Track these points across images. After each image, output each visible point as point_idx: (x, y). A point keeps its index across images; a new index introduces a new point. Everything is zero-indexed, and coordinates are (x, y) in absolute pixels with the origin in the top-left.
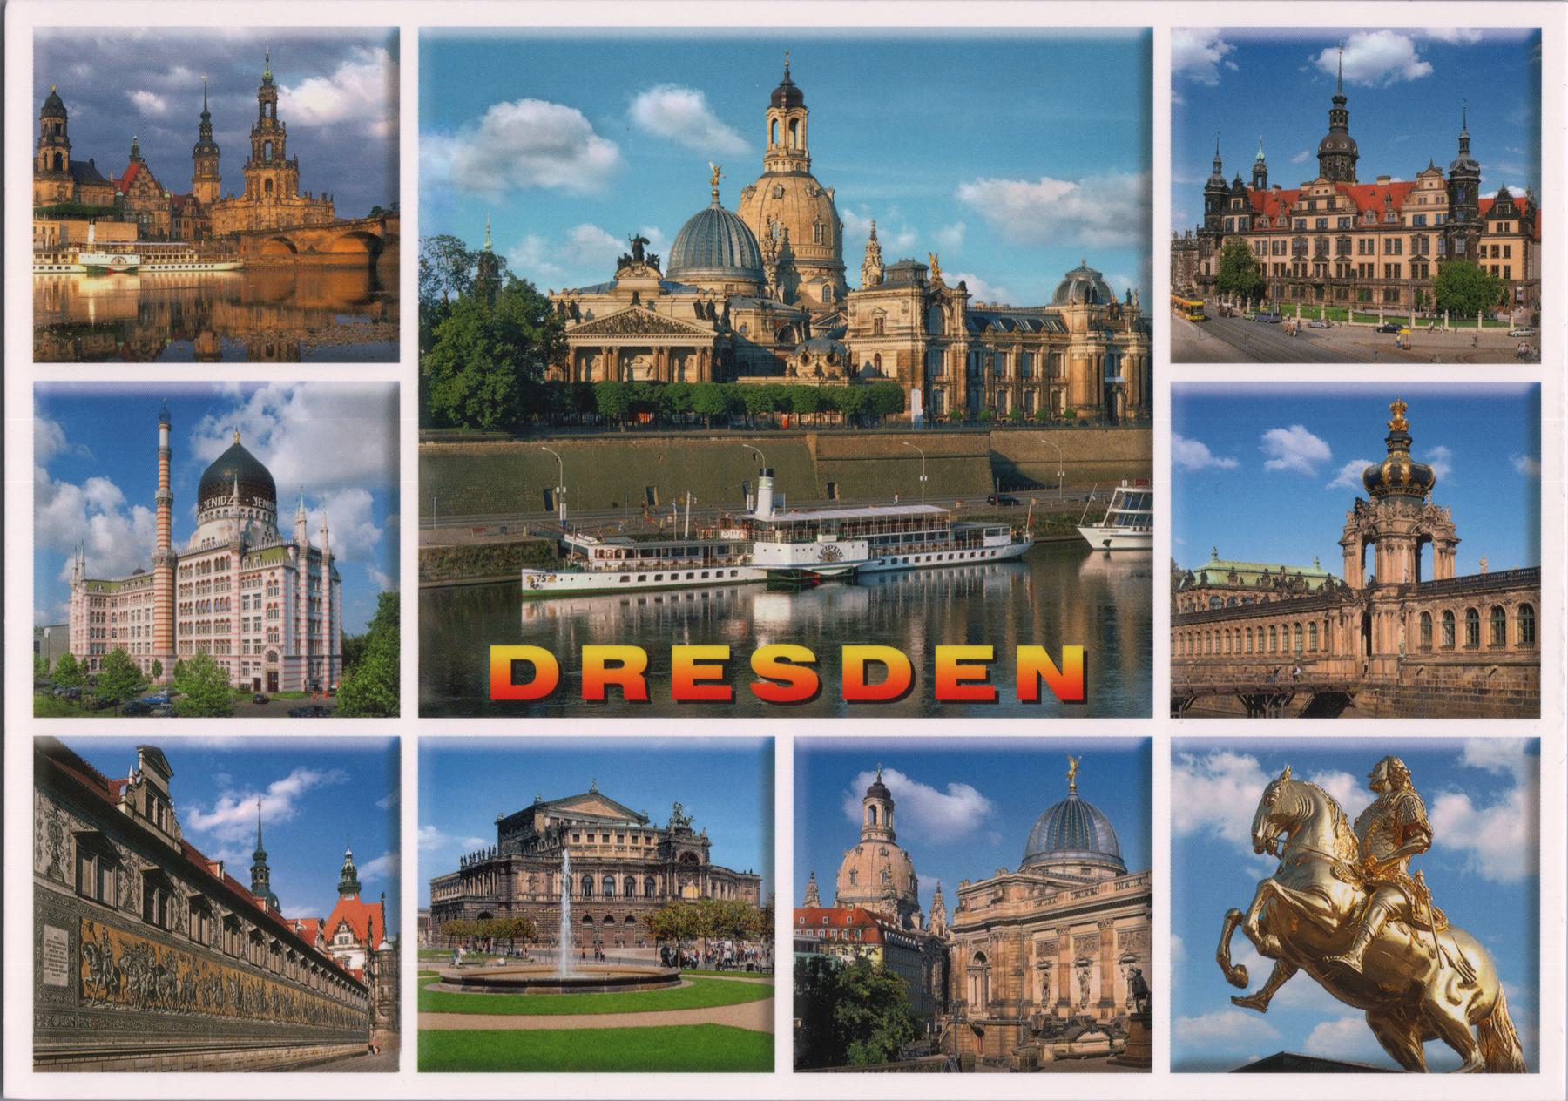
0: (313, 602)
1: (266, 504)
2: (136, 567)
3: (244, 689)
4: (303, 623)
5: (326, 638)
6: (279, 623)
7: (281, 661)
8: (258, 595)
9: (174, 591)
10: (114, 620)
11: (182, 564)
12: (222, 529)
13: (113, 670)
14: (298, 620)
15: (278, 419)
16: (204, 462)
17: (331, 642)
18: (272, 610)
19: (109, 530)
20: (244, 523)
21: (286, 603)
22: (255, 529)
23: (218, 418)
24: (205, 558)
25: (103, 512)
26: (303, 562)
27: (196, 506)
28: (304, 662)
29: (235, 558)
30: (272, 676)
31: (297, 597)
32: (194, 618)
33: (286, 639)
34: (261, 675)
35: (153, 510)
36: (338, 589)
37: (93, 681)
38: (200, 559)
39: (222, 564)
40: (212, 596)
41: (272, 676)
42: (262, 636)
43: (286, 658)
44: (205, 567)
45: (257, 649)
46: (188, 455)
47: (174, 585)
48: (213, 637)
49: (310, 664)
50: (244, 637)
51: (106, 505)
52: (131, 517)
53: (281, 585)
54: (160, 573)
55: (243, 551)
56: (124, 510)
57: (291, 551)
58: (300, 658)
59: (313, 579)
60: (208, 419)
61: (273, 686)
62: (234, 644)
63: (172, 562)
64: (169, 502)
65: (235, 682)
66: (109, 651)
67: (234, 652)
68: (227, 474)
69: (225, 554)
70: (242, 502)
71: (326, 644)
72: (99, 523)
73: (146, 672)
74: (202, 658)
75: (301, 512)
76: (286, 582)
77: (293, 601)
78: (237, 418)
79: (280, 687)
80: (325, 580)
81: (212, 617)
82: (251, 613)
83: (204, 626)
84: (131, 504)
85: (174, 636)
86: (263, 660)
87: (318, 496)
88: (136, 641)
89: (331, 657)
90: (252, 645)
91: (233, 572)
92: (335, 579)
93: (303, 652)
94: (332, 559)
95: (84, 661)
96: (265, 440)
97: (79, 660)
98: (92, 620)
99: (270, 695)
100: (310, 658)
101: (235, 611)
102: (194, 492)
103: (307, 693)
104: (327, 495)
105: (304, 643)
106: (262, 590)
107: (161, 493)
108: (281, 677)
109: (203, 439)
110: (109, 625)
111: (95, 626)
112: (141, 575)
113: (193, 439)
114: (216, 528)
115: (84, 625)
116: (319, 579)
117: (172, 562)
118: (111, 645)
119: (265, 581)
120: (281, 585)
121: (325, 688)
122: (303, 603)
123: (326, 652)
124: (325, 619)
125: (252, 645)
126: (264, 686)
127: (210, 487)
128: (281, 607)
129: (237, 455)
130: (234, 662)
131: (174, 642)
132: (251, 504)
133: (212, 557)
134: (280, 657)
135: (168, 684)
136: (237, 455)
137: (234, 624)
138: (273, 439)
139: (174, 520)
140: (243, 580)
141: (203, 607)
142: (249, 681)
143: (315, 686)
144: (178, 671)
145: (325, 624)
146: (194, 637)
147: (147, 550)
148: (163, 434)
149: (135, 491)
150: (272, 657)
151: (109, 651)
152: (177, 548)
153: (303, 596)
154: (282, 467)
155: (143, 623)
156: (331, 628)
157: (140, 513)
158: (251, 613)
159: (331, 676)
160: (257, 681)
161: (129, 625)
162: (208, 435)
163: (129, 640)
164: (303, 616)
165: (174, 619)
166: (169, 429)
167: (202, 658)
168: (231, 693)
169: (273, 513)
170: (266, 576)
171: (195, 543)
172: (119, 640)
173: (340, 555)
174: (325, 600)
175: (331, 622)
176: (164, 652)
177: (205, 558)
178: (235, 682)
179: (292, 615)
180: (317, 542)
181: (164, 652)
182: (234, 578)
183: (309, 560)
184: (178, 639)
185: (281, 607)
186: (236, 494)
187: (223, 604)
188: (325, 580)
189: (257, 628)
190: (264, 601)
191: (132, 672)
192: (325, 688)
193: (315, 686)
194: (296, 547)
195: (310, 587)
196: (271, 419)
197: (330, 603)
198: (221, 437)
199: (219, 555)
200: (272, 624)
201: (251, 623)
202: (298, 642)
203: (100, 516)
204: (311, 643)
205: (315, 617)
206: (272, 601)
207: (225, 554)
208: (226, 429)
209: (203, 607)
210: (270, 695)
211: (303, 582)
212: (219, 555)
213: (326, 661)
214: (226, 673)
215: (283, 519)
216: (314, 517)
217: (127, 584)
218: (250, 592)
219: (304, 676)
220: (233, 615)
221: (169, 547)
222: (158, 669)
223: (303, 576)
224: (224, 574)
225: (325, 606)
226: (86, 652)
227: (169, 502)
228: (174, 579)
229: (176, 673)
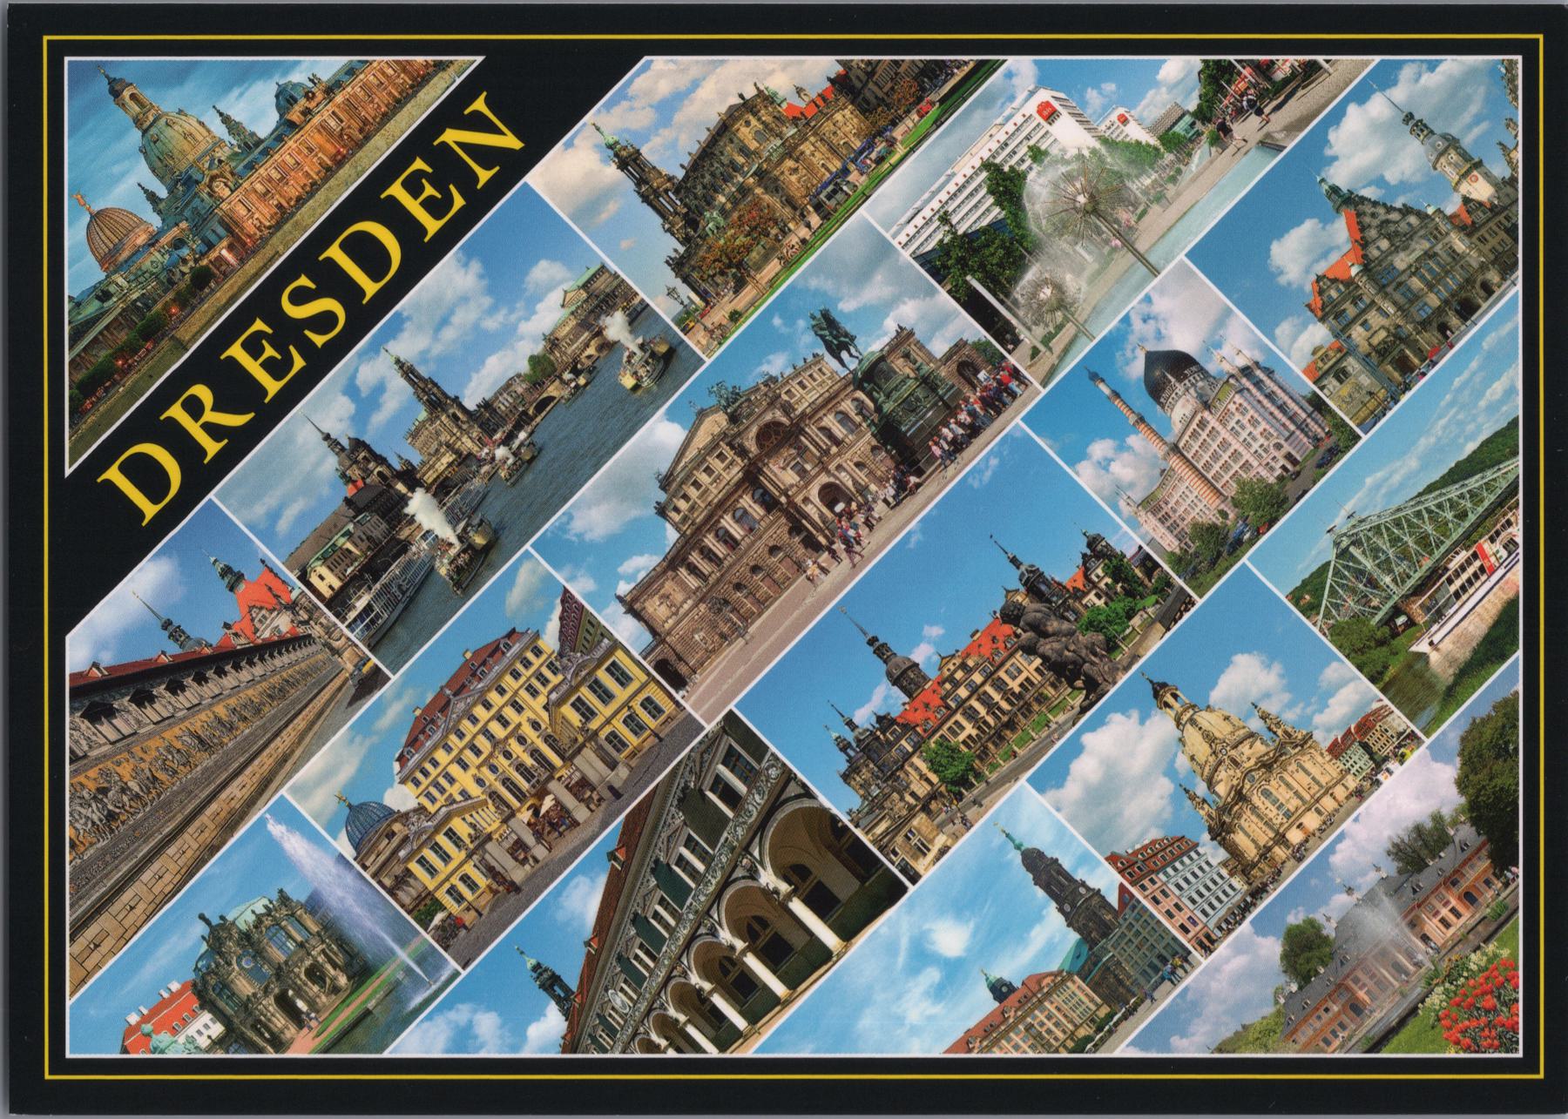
0: (1270, 396)
1: (1194, 369)
2: (1158, 472)
3: (1280, 479)
4: (1277, 412)
5: (1296, 408)
6: (1264, 425)
7: (1285, 445)
11: (1181, 445)
13: (1201, 538)
15: (1155, 318)
20: (1192, 391)
29: (1206, 414)
30: (1289, 457)
32: (1217, 467)
34: (1282, 462)
35: (1137, 433)
36: (1277, 376)
37: (1196, 555)
38: (1189, 433)
39: (1203, 424)
40: (1214, 446)
41: (1289, 457)
42: (1262, 440)
44: (1194, 435)
45: (1266, 451)
48: (1236, 467)
49: (1302, 430)
51: (1110, 454)
52: (1129, 449)
54: (1174, 462)
55: (1207, 406)
56: (1122, 447)
57: (1232, 381)
59: (1258, 384)
60: (1118, 354)
61: (1294, 462)
62: (1251, 460)
63: (1175, 449)
64: (1141, 419)
65: (1272, 480)
67: (1255, 464)
68: (1157, 373)
69: (1198, 418)
70: (1180, 381)
72: (1116, 468)
73: (1219, 521)
74: (1242, 485)
75: (1217, 354)
78: (1133, 339)
81: (1225, 457)
82: (1244, 435)
83: (1226, 467)
86: (1274, 453)
91: (1213, 422)
92: (1269, 372)
93: (1292, 427)
94: (1257, 363)
96: (1159, 336)
97: (1177, 551)
100: (1299, 427)
101: (1234, 442)
103: (1316, 447)
105: (1288, 423)
106: (1238, 416)
107: (1132, 419)
109: (1127, 369)
110: (1175, 517)
114: (1182, 407)
115: (1162, 530)
117: (1175, 449)
122: (1266, 402)
123: (1304, 415)
124: (1286, 398)
126: (1289, 466)
127: (1156, 390)
129: (1153, 359)
130: (1260, 469)
132: (1186, 377)
133: (1194, 426)
135: (1237, 517)
136: (1153, 359)
137: (1241, 449)
141: (1216, 457)
142: (1279, 472)
143: (1317, 440)
144: (1236, 503)
145: (1289, 401)
146: (1227, 477)
147: (1155, 456)
150: (1278, 446)
152: (1170, 439)
153: (1261, 398)
154: (1183, 340)
155: (1192, 497)
158: (1244, 435)
160: (1283, 467)
167: (1242, 485)
169: (1202, 370)
170: (1232, 407)
172: (1188, 519)
174: (1276, 389)
178: (1272, 480)
180: (1241, 362)
187: (1224, 445)
189: (1254, 439)
190: (1245, 422)
191: (1212, 529)
193: (1317, 440)
194: (1232, 376)
195: (1260, 389)
196: (1152, 322)
200: (1260, 429)
204: (1291, 419)
206: (1248, 417)
207: (1198, 418)
209: (1216, 457)
211: (1254, 390)
214: (1261, 480)
215: (1211, 368)
216: (1226, 350)
218: (1232, 424)
222: (1224, 514)
223: (1251, 387)
225: (1279, 392)
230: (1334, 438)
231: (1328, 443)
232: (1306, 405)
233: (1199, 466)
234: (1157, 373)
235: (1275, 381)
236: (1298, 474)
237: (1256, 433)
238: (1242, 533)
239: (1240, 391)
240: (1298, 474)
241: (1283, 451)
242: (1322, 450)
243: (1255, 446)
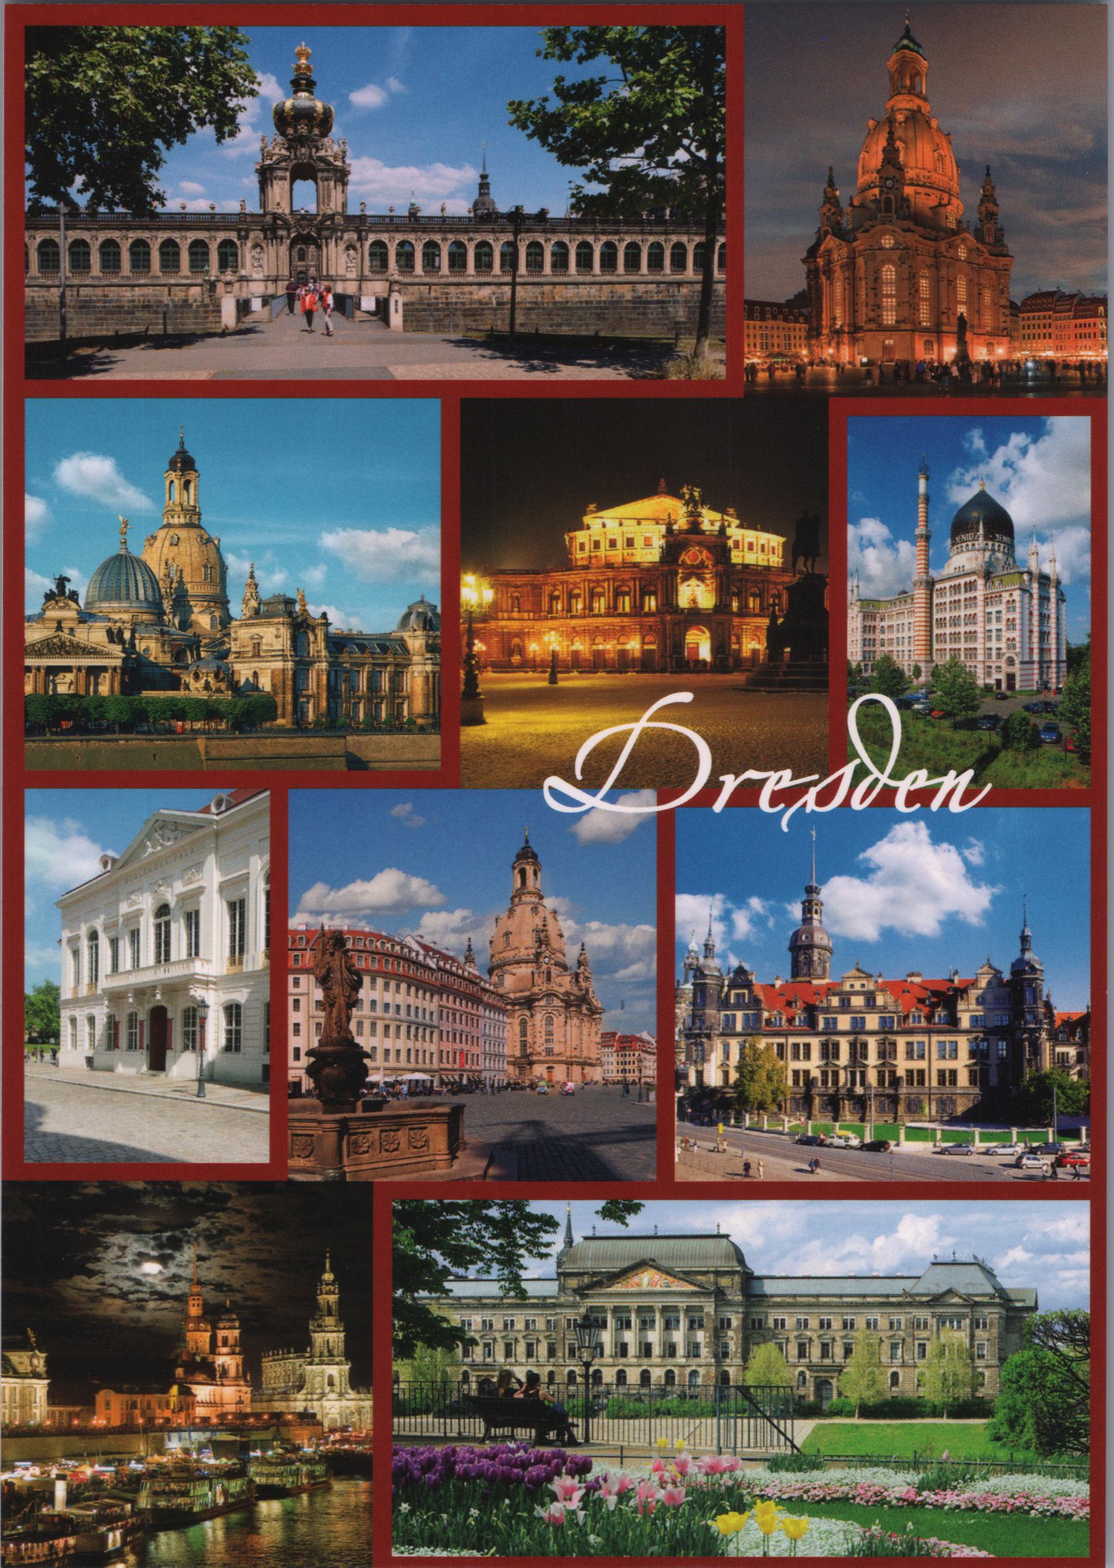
0: (1044, 618)
1: (1005, 539)
2: (900, 589)
3: (988, 688)
5: (1054, 646)
6: (1016, 634)
7: (1017, 666)
8: (999, 612)
9: (931, 608)
10: (883, 632)
11: (938, 586)
12: (969, 559)
13: (882, 673)
14: (1031, 631)
15: (1015, 471)
16: (956, 505)
17: (1058, 650)
18: (1011, 624)
19: (879, 560)
20: (988, 554)
21: (1022, 619)
22: (997, 559)
23: (967, 470)
24: (956, 582)
25: (873, 546)
26: (1035, 585)
27: (949, 542)
28: (1036, 666)
29: (980, 582)
30: (1011, 677)
31: (1031, 613)
32: (948, 630)
33: (1022, 648)
34: (1002, 676)
35: (913, 543)
36: (1064, 606)
39: (970, 586)
41: (1011, 677)
42: (1003, 645)
43: (1022, 663)
44: (956, 589)
45: (999, 656)
46: (943, 500)
47: (931, 603)
48: (962, 645)
49: (1041, 668)
50: (988, 645)
51: (877, 540)
52: (896, 550)
53: (1018, 604)
54: (920, 594)
55: (988, 576)
56: (891, 544)
57: (1026, 577)
58: (1032, 662)
59: (1044, 599)
60: (959, 470)
61: (1011, 686)
62: (980, 652)
63: (930, 585)
64: (927, 538)
65: (980, 682)
66: (878, 658)
67: (980, 658)
68: (975, 514)
69: (973, 578)
70: (986, 538)
71: (1054, 651)
72: (871, 554)
73: (908, 673)
74: (954, 663)
75: (1034, 545)
76: (1022, 601)
77: (1027, 617)
78: (982, 469)
79: (1017, 687)
80: (1053, 600)
81: (962, 629)
82: (994, 626)
83: (955, 637)
84: (897, 539)
85: (931, 645)
86: (1003, 664)
87: (1047, 532)
88: (900, 648)
89: (1058, 662)
90: (994, 652)
91: (980, 592)
92: (1061, 599)
93: (1036, 658)
94: (1058, 582)
95: (859, 665)
96: (1005, 487)
98: (864, 631)
99: (1009, 693)
100: (1041, 662)
101: (980, 624)
102: (948, 529)
103: (1039, 692)
104: (1054, 532)
105: (1036, 651)
106: (1002, 607)
107: (920, 530)
108: (1018, 678)
110: (879, 636)
111: (868, 636)
112: (904, 596)
113: (947, 486)
114: (966, 559)
116: (1049, 599)
117: (930, 585)
118: (880, 651)
119: (1004, 601)
120: (1018, 604)
121: (1053, 687)
122: (1036, 618)
123: (1054, 658)
124: (1053, 631)
125: (994, 652)
126: (1004, 686)
127: (961, 527)
128: (1018, 622)
129: (983, 501)
130: (980, 666)
131: (931, 650)
132: (993, 539)
133: (962, 581)
134: (1017, 661)
136: (983, 501)
137: (980, 635)
138: (1011, 487)
139: (931, 552)
140: (988, 600)
141: (955, 621)
142: (991, 681)
143: (1045, 686)
144: (935, 673)
145: (1053, 636)
146: (948, 646)
147: (909, 575)
148: (922, 485)
149: (900, 528)
150: (1011, 662)
151: (878, 658)
152: (934, 574)
153: (1036, 613)
154: (1020, 509)
155: (906, 634)
156: (1058, 639)
157: (904, 546)
159: (1058, 678)
160: (999, 682)
161: (894, 636)
162: (960, 483)
163: (895, 648)
164: (1036, 629)
165: (931, 631)
166: (927, 478)
167: (954, 663)
168: (978, 692)
169: (1011, 547)
170: (1006, 597)
171: (949, 570)
172: (886, 649)
173: (1065, 579)
174: (1053, 616)
175: (1058, 634)
176: (923, 658)
177: (956, 582)
178: (980, 682)
179: (1027, 629)
180: (1047, 569)
181: (923, 658)
182: (980, 598)
183: (1040, 583)
184: (935, 646)
185: (1018, 622)
186: (981, 531)
188: (1053, 600)
189: (999, 639)
190: (1004, 617)
192: (1053, 687)
193: (1045, 686)
194: (1030, 573)
195: (1041, 605)
196: (1010, 471)
197: (1058, 619)
198: (969, 485)
199: (968, 579)
200: (1011, 635)
201: (994, 634)
202: (1031, 650)
203: (871, 549)
205: (1046, 629)
207: (973, 578)
208: (973, 479)
209: (955, 621)
210: (1009, 693)
211: (1035, 602)
212: (968, 579)
213: (1054, 665)
214: (972, 675)
215: (1020, 551)
216: (1045, 549)
217: (892, 603)
218: (993, 609)
219: (1036, 677)
220: (979, 628)
221: (927, 573)
222: (917, 672)
223: (1036, 596)
224: (972, 595)
225: (1053, 620)
226: (860, 658)
227: (927, 538)
228: (931, 599)
229: (933, 675)
230: (1059, 697)
231: (1051, 697)
232: (1064, 652)
233: (936, 616)
234: (975, 514)
235: (1058, 609)
236: (1004, 697)
237: (1006, 635)
238: (917, 700)
239: (1023, 590)
240: (1004, 697)
241: (1011, 670)
242: (1041, 697)
243: (994, 645)
